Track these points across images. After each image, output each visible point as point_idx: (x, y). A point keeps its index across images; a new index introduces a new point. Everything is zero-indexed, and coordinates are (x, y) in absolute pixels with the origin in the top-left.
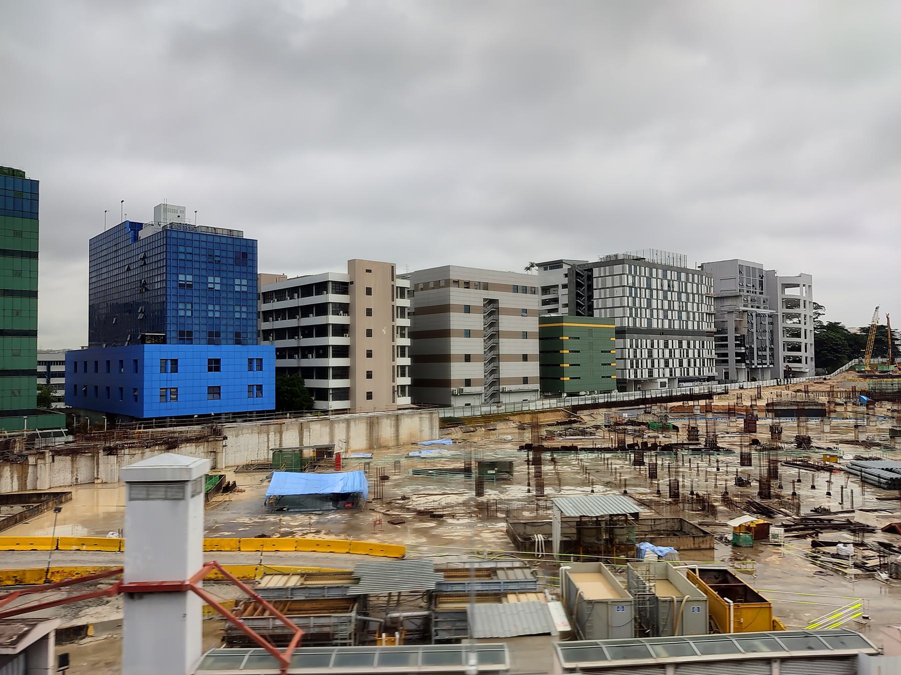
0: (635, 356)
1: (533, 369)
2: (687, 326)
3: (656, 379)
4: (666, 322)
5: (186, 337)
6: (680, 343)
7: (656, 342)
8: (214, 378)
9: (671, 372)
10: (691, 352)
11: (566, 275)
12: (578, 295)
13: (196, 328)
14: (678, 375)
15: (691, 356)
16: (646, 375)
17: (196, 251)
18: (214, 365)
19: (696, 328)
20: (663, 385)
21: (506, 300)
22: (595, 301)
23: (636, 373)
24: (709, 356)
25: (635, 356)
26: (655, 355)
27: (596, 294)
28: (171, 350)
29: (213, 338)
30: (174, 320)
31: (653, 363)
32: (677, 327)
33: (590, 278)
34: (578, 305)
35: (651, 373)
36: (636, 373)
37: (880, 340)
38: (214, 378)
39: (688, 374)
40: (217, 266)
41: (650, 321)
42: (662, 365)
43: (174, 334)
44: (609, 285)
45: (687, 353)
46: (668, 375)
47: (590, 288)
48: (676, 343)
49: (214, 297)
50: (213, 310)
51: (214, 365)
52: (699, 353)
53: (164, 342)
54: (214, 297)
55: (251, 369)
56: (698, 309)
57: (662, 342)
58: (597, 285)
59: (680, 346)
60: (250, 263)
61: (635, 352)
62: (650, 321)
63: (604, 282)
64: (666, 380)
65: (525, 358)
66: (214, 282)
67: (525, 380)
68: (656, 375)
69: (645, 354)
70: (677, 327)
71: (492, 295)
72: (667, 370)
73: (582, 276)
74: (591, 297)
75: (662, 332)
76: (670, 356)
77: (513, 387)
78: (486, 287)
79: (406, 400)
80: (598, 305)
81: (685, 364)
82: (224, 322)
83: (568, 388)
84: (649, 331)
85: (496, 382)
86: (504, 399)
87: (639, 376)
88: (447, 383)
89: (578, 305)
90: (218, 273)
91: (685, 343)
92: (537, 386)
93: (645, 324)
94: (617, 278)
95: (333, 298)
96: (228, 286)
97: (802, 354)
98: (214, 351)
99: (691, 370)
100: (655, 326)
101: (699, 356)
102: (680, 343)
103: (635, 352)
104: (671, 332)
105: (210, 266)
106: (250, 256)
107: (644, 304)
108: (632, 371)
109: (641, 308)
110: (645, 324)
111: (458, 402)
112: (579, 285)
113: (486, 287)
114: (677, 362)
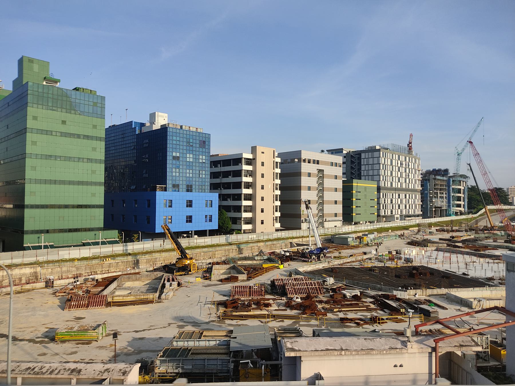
0: (385, 202)
1: (339, 209)
4: (399, 184)
5: (176, 187)
6: (406, 196)
8: (189, 211)
10: (410, 200)
11: (345, 157)
12: (352, 168)
13: (181, 182)
14: (404, 213)
15: (410, 203)
16: (389, 213)
17: (181, 139)
18: (190, 204)
20: (397, 219)
21: (329, 170)
22: (362, 172)
23: (385, 212)
25: (385, 202)
27: (363, 168)
28: (169, 194)
29: (189, 189)
30: (171, 178)
31: (393, 206)
32: (404, 187)
33: (360, 158)
34: (352, 173)
37: (499, 196)
38: (189, 211)
40: (191, 148)
41: (392, 184)
43: (171, 186)
44: (371, 162)
46: (399, 213)
47: (360, 164)
48: (404, 195)
49: (190, 166)
50: (189, 173)
51: (190, 204)
53: (166, 190)
54: (190, 166)
55: (207, 206)
58: (364, 162)
60: (207, 147)
61: (385, 201)
63: (368, 161)
64: (399, 216)
65: (336, 202)
66: (190, 157)
67: (336, 215)
68: (394, 213)
69: (389, 202)
71: (320, 167)
72: (399, 210)
73: (354, 158)
74: (360, 169)
75: (396, 189)
77: (330, 219)
78: (318, 162)
79: (278, 225)
80: (364, 173)
82: (194, 179)
83: (354, 220)
84: (391, 189)
85: (322, 216)
86: (326, 224)
88: (299, 216)
89: (352, 173)
90: (191, 152)
91: (407, 195)
92: (341, 218)
94: (376, 159)
95: (245, 167)
96: (196, 159)
97: (462, 203)
98: (189, 196)
99: (410, 210)
102: (406, 196)
104: (401, 190)
105: (188, 148)
106: (207, 143)
108: (383, 211)
110: (389, 185)
111: (304, 226)
112: (352, 162)
113: (318, 162)
114: (404, 206)
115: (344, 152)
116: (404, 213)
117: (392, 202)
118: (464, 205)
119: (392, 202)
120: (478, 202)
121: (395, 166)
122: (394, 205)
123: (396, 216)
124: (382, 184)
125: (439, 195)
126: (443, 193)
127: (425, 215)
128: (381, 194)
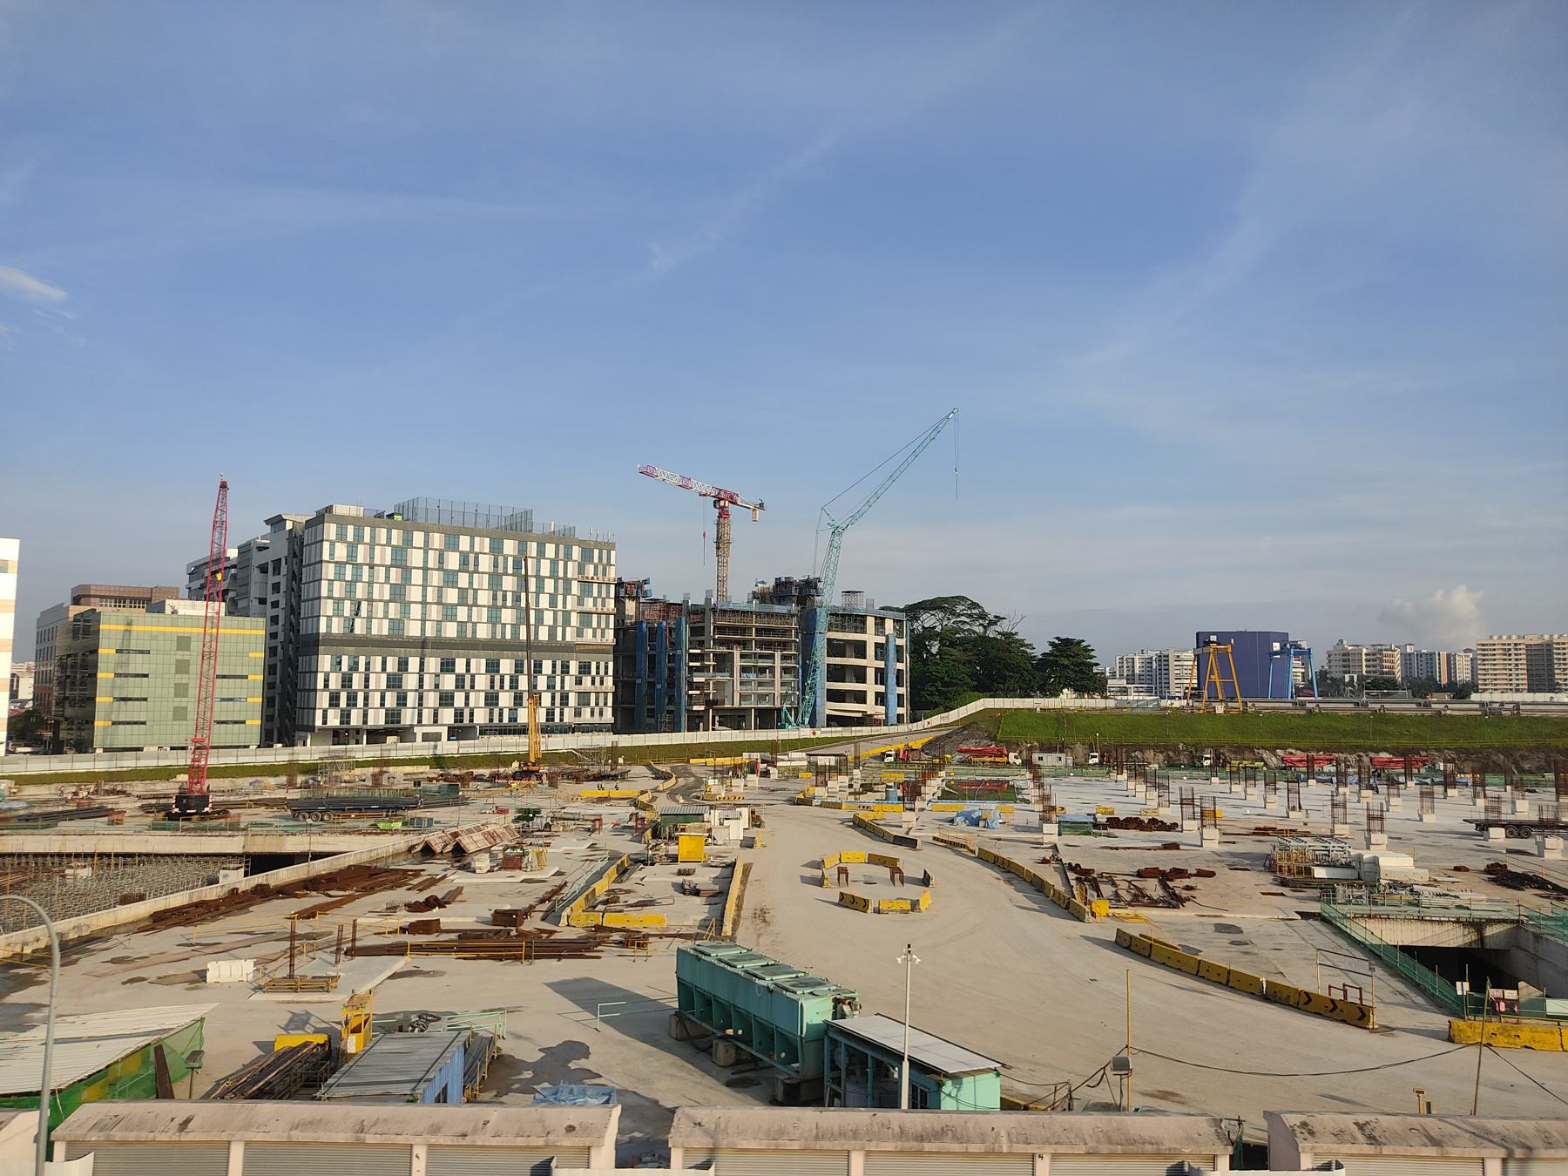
2: (516, 632)
3: (412, 726)
7: (414, 663)
9: (459, 715)
14: (481, 717)
19: (543, 635)
20: (426, 737)
23: (346, 717)
24: (581, 688)
26: (410, 681)
31: (402, 700)
35: (393, 716)
36: (346, 717)
39: (513, 719)
41: (397, 625)
42: (432, 700)
45: (514, 683)
48: (478, 665)
52: (551, 678)
56: (553, 603)
57: (433, 664)
59: (493, 667)
61: (347, 682)
62: (397, 625)
64: (444, 731)
68: (408, 717)
69: (379, 681)
70: (483, 632)
75: (439, 644)
76: (460, 684)
81: (505, 699)
84: (395, 643)
87: (355, 719)
91: (506, 666)
93: (381, 628)
100: (413, 630)
101: (551, 687)
103: (347, 682)
104: (469, 645)
107: (382, 592)
109: (370, 601)
115: (289, 526)
116: (481, 717)
117: (394, 682)
118: (881, 699)
119: (394, 682)
120: (945, 684)
121: (425, 569)
122: (412, 699)
123: (419, 731)
124: (329, 623)
125: (738, 662)
126: (772, 657)
127: (615, 729)
128: (325, 662)
